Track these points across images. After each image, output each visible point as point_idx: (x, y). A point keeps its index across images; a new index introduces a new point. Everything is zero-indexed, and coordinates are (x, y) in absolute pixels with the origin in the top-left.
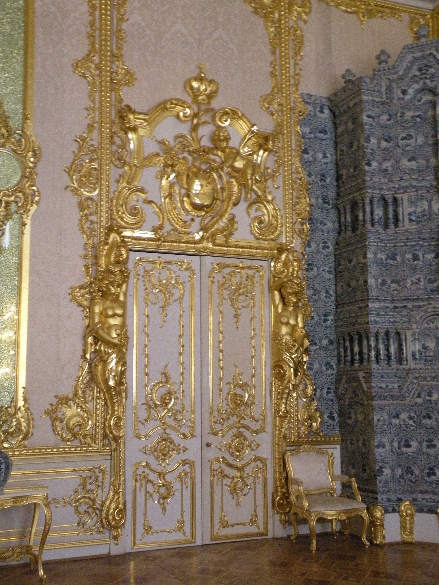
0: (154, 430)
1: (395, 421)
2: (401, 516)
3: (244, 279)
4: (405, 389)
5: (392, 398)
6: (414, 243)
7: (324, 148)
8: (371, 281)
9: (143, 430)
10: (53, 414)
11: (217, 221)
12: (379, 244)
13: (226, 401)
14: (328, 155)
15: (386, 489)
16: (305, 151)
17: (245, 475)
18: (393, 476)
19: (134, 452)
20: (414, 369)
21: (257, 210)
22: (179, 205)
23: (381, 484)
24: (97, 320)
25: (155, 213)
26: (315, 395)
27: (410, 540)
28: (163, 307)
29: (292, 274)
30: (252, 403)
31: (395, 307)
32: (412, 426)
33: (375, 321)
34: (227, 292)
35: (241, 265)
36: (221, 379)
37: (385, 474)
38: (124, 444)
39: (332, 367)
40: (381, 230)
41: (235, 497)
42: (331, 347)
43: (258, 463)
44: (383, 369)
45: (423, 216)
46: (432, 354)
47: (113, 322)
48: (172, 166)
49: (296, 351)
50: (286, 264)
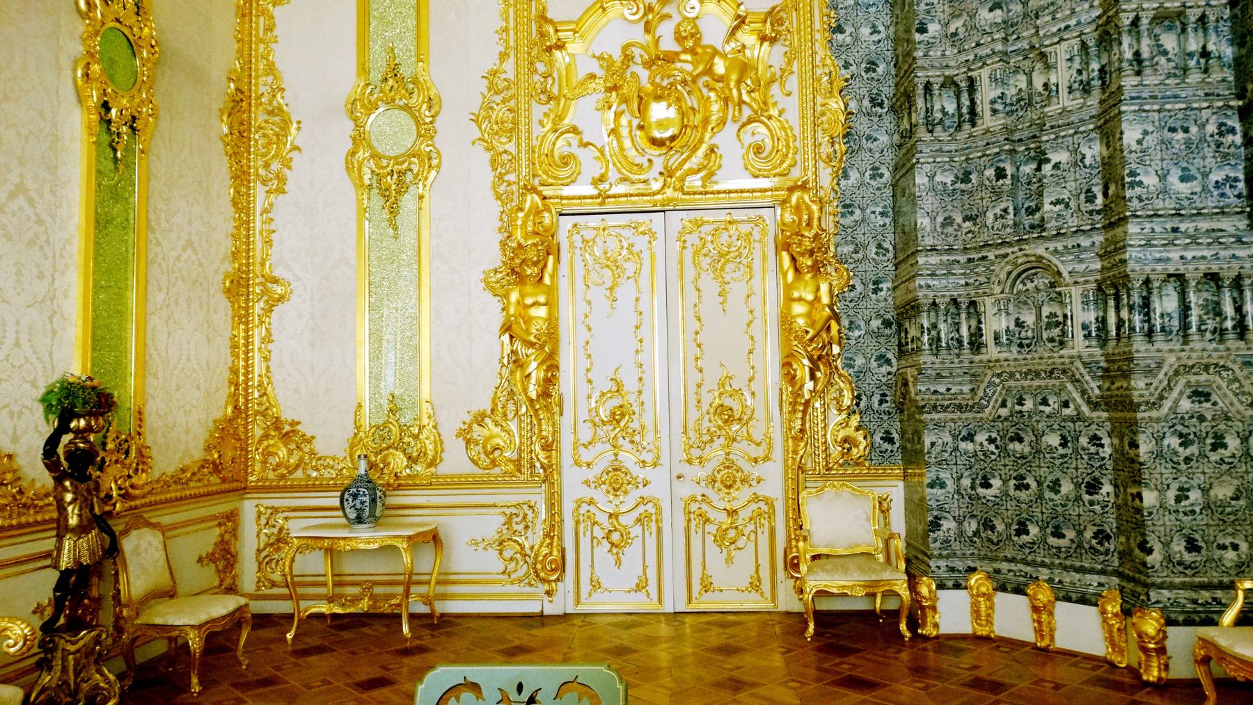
0: (601, 457)
1: (969, 446)
2: (972, 596)
3: (735, 238)
4: (981, 393)
5: (960, 408)
6: (997, 150)
7: (872, 19)
8: (923, 222)
9: (586, 456)
10: (465, 435)
11: (689, 157)
12: (938, 160)
13: (707, 417)
14: (881, 28)
15: (945, 553)
16: (839, 29)
17: (740, 522)
18: (961, 533)
19: (573, 484)
20: (997, 361)
21: (753, 134)
22: (627, 143)
23: (938, 544)
24: (512, 311)
25: (597, 158)
26: (858, 405)
27: (985, 633)
28: (611, 289)
29: (809, 224)
30: (750, 419)
31: (970, 260)
32: (993, 453)
33: (929, 286)
34: (708, 260)
35: (728, 218)
36: (699, 386)
37: (944, 528)
38: (559, 474)
39: (888, 362)
40: (944, 136)
41: (725, 551)
42: (888, 331)
43: (761, 504)
44: (942, 363)
45: (1019, 101)
46: (1030, 334)
47: (534, 312)
48: (615, 88)
49: (811, 340)
50: (797, 209)
